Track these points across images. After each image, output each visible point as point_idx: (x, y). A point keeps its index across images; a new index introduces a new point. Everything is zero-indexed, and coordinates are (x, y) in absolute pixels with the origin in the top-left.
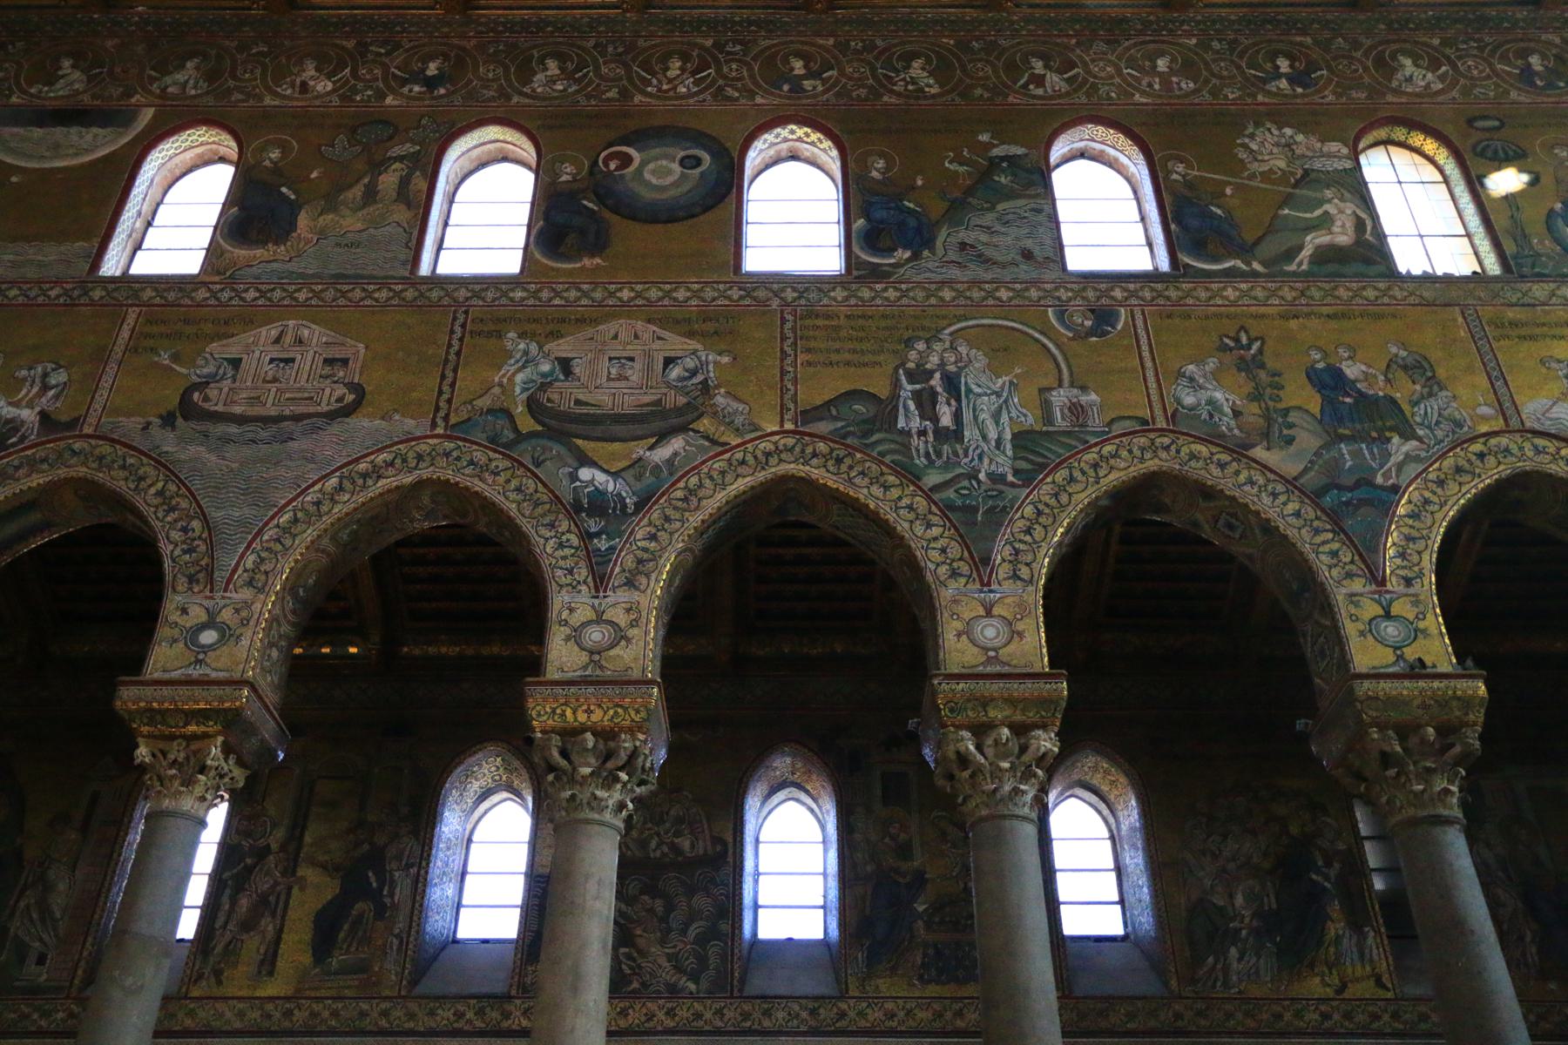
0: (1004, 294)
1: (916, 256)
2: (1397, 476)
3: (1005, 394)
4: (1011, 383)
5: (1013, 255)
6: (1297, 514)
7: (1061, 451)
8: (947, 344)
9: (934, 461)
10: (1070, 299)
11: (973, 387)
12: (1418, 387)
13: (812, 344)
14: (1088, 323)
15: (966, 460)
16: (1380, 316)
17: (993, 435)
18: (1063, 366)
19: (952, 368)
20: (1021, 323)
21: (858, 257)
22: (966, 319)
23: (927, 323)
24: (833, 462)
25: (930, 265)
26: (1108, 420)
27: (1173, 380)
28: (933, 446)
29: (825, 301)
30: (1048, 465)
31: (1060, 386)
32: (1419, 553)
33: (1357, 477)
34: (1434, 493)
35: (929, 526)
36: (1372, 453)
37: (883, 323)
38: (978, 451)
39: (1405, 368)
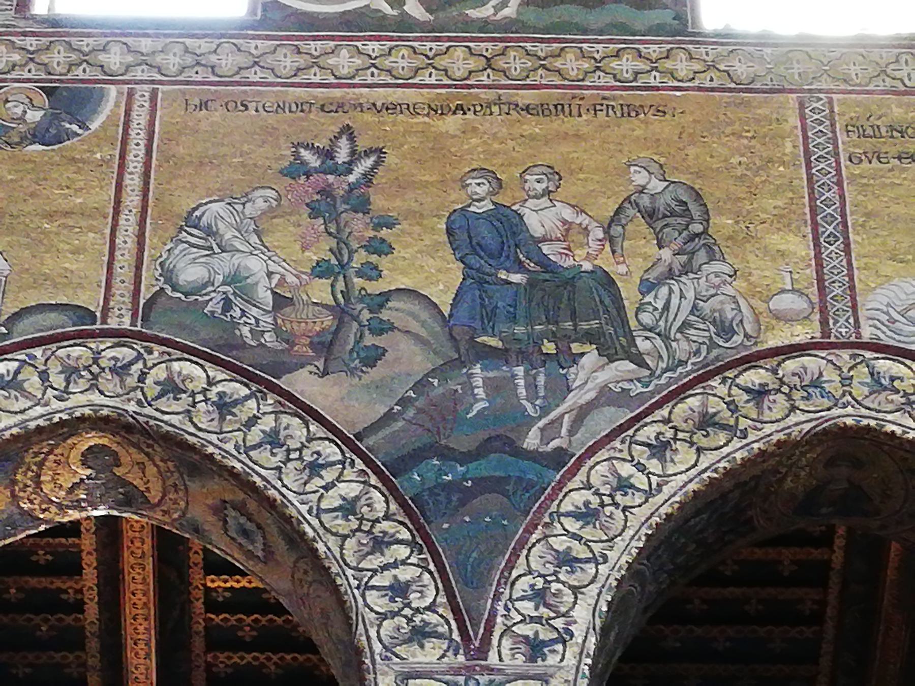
2: (572, 432)
6: (348, 508)
12: (666, 254)
14: (34, 116)
16: (630, 111)
27: (172, 231)
32: (576, 590)
33: (482, 435)
34: (641, 468)
36: (532, 386)
39: (651, 215)
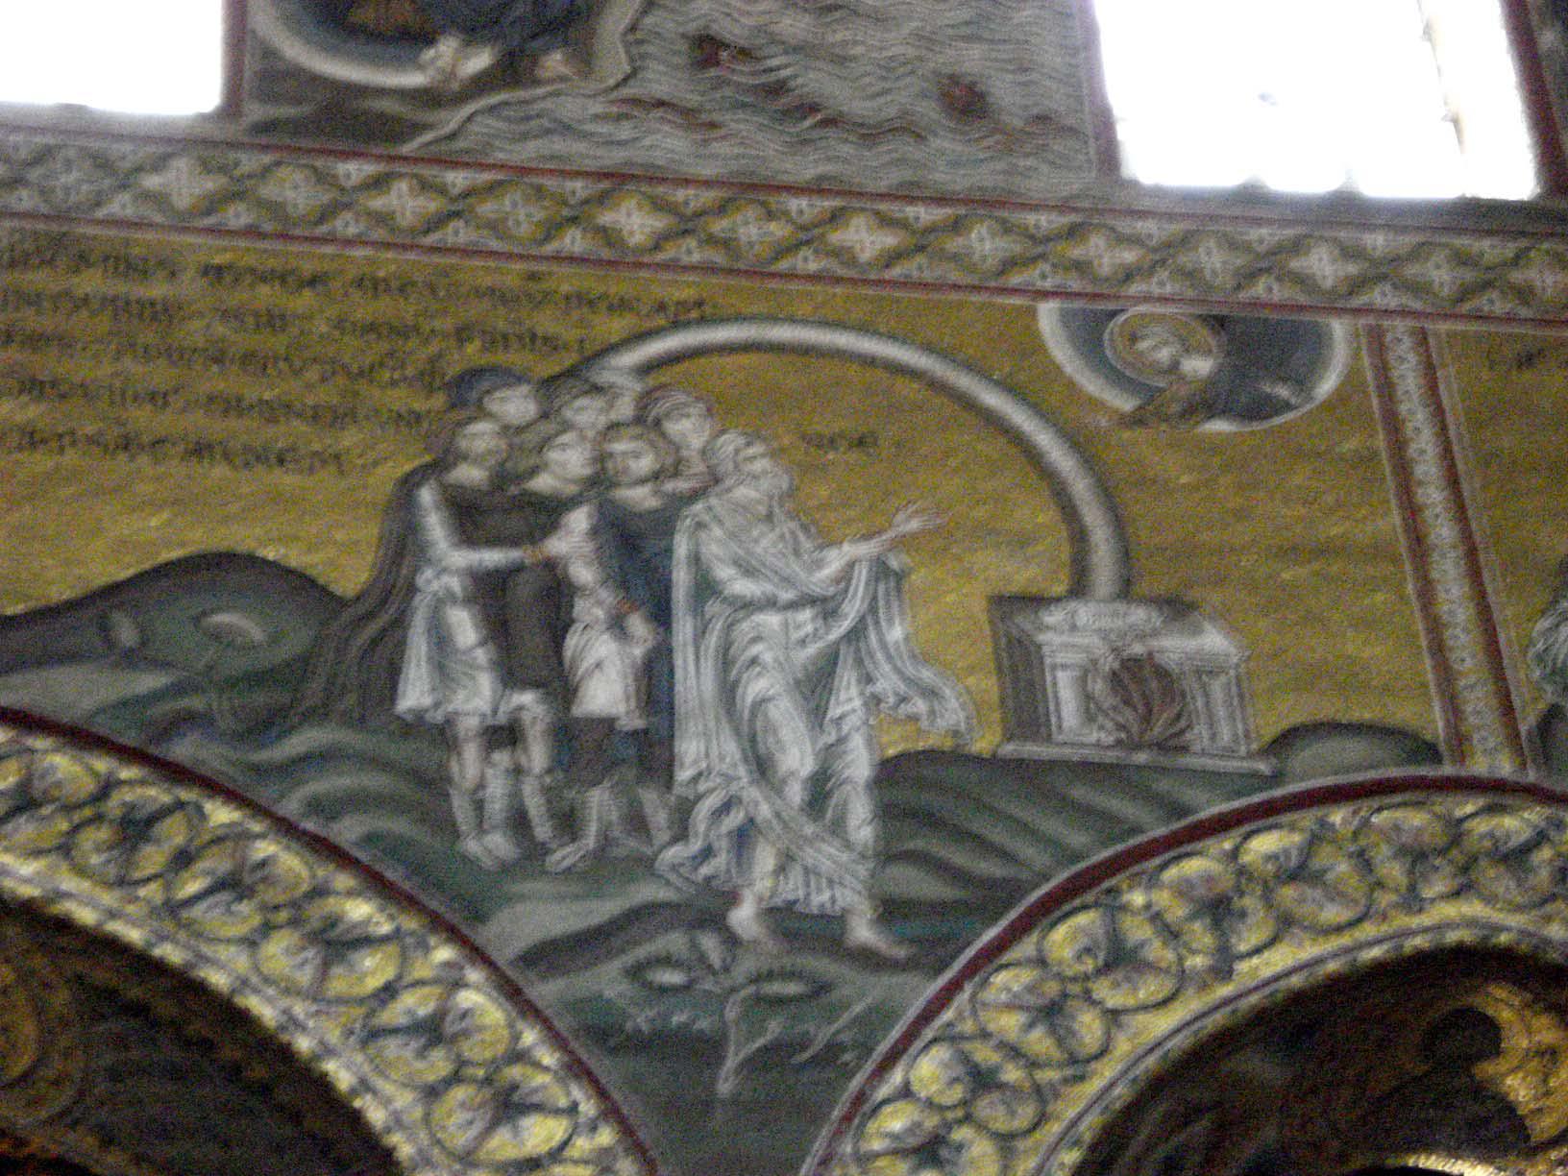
0: (864, 238)
1: (512, 70)
3: (852, 609)
4: (881, 570)
5: (909, 97)
7: (1077, 839)
8: (625, 409)
9: (541, 851)
10: (1129, 275)
11: (723, 572)
13: (48, 364)
14: (1200, 366)
15: (675, 853)
17: (797, 758)
18: (1093, 516)
19: (641, 498)
20: (928, 348)
21: (269, 53)
22: (703, 321)
23: (546, 322)
24: (103, 833)
25: (570, 108)
26: (1270, 732)
28: (549, 793)
29: (121, 205)
30: (1013, 890)
31: (1079, 588)
35: (509, 1106)
37: (365, 309)
38: (734, 819)
